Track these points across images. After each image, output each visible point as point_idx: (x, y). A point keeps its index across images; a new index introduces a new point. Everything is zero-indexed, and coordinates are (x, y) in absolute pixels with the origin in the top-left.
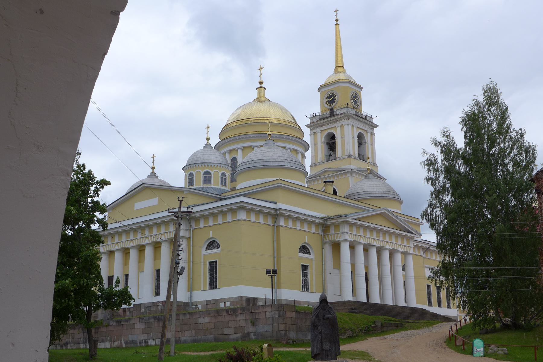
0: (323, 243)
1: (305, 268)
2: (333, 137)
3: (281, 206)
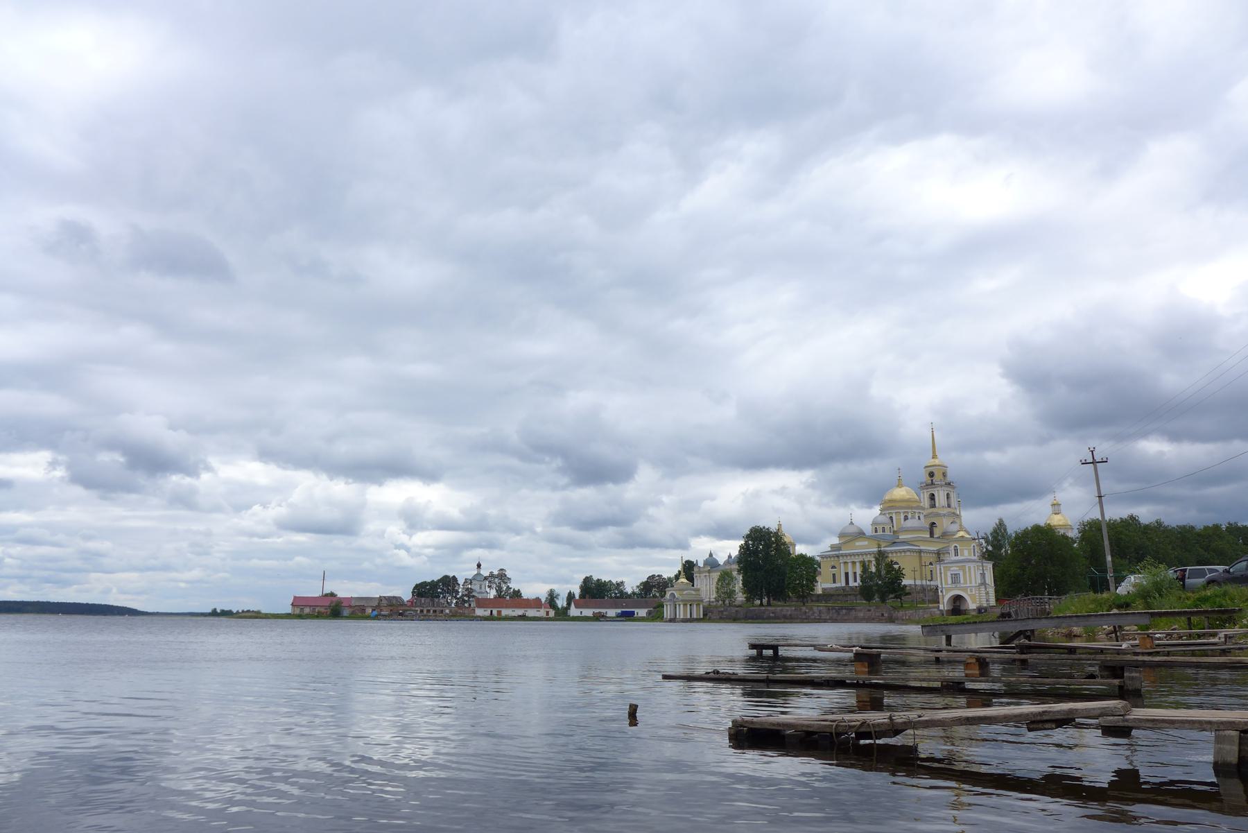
1: (931, 571)
2: (933, 495)
3: (922, 548)
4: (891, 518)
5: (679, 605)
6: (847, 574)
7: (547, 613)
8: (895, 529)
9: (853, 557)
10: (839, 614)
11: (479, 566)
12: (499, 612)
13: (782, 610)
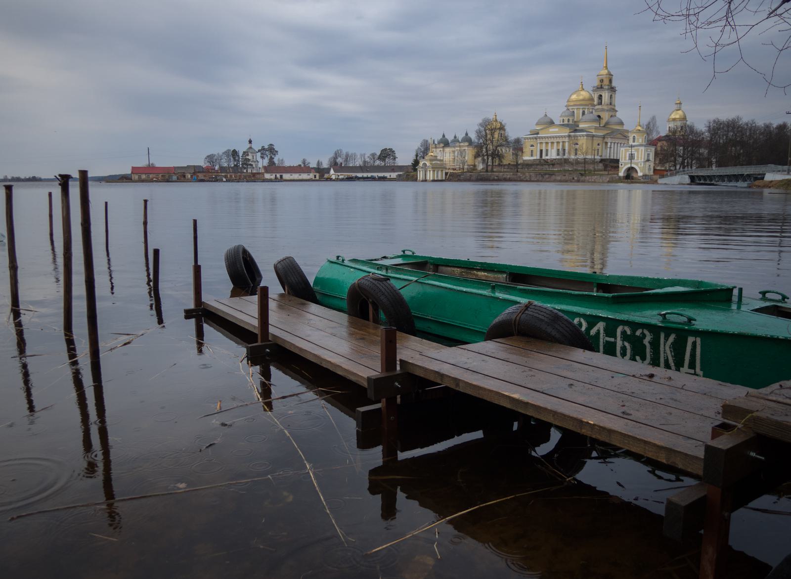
0: (603, 142)
2: (601, 96)
3: (594, 134)
4: (574, 112)
5: (430, 171)
6: (541, 151)
7: (315, 177)
8: (575, 120)
9: (558, 139)
10: (543, 178)
11: (250, 142)
12: (281, 176)
13: (503, 175)
